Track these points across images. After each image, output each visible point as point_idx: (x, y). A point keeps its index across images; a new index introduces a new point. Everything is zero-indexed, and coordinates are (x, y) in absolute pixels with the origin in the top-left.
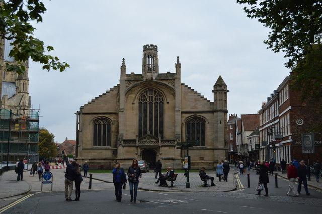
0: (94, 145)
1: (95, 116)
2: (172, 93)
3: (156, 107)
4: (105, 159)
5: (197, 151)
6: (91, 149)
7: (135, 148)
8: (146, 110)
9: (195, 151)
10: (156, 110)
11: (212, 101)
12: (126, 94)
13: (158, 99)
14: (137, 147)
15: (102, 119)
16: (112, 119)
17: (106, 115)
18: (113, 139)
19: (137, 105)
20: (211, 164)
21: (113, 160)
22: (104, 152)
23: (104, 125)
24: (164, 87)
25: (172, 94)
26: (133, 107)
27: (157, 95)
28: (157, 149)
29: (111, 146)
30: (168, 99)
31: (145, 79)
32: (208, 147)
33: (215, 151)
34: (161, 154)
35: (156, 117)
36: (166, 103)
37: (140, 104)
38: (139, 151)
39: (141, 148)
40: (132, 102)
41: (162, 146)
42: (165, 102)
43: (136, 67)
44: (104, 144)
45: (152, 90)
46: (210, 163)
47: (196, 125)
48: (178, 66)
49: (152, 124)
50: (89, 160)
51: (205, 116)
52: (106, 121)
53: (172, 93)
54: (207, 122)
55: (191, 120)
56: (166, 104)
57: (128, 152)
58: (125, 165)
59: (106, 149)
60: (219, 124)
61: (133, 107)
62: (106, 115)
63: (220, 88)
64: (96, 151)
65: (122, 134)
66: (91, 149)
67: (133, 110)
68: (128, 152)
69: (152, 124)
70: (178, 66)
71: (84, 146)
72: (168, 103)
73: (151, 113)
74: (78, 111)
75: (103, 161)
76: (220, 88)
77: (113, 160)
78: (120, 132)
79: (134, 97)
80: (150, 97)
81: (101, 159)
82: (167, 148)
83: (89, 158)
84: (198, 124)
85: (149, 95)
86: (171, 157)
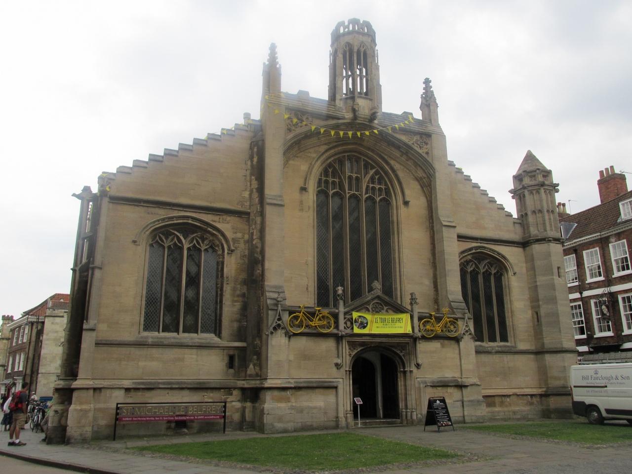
0: (147, 328)
1: (162, 213)
2: (420, 173)
3: (371, 212)
4: (200, 387)
5: (496, 358)
6: (140, 344)
7: (331, 344)
8: (338, 217)
9: (490, 356)
10: (372, 222)
11: (515, 216)
12: (284, 154)
13: (373, 188)
14: (338, 338)
15: (187, 229)
16: (229, 235)
17: (207, 218)
18: (230, 309)
19: (311, 197)
20: (535, 400)
21: (228, 390)
22: (190, 356)
23: (195, 251)
24: (397, 153)
25: (417, 179)
26: (301, 202)
27: (372, 180)
28: (403, 346)
29: (218, 334)
30: (407, 192)
31: (349, 116)
32: (522, 346)
33: (548, 357)
34: (418, 366)
35: (372, 243)
36: (400, 202)
37: (322, 193)
38: (347, 356)
39: (352, 345)
40: (300, 183)
41: (423, 338)
42: (397, 200)
43: (310, 79)
44: (191, 328)
45: (358, 160)
46: (532, 396)
47: (480, 279)
48: (428, 102)
49: (357, 262)
50: (128, 390)
51: (503, 253)
52: (203, 240)
53: (420, 173)
54: (510, 273)
55: (468, 262)
56: (402, 206)
57: (305, 357)
58: (301, 411)
59: (201, 347)
60: (556, 277)
61: (301, 202)
62: (207, 218)
63: (534, 181)
64: (155, 352)
65: (279, 290)
66: (140, 344)
67: (302, 210)
68: (305, 357)
69: (357, 262)
70: (428, 102)
71: (104, 331)
72: (406, 203)
73: (355, 229)
74: (87, 189)
75: (186, 397)
76: (534, 181)
77: (228, 390)
78: (272, 280)
79: (304, 167)
80: (350, 178)
81: (181, 388)
82: (435, 345)
83: (127, 384)
84: (487, 275)
85: (348, 174)
86: (449, 374)
